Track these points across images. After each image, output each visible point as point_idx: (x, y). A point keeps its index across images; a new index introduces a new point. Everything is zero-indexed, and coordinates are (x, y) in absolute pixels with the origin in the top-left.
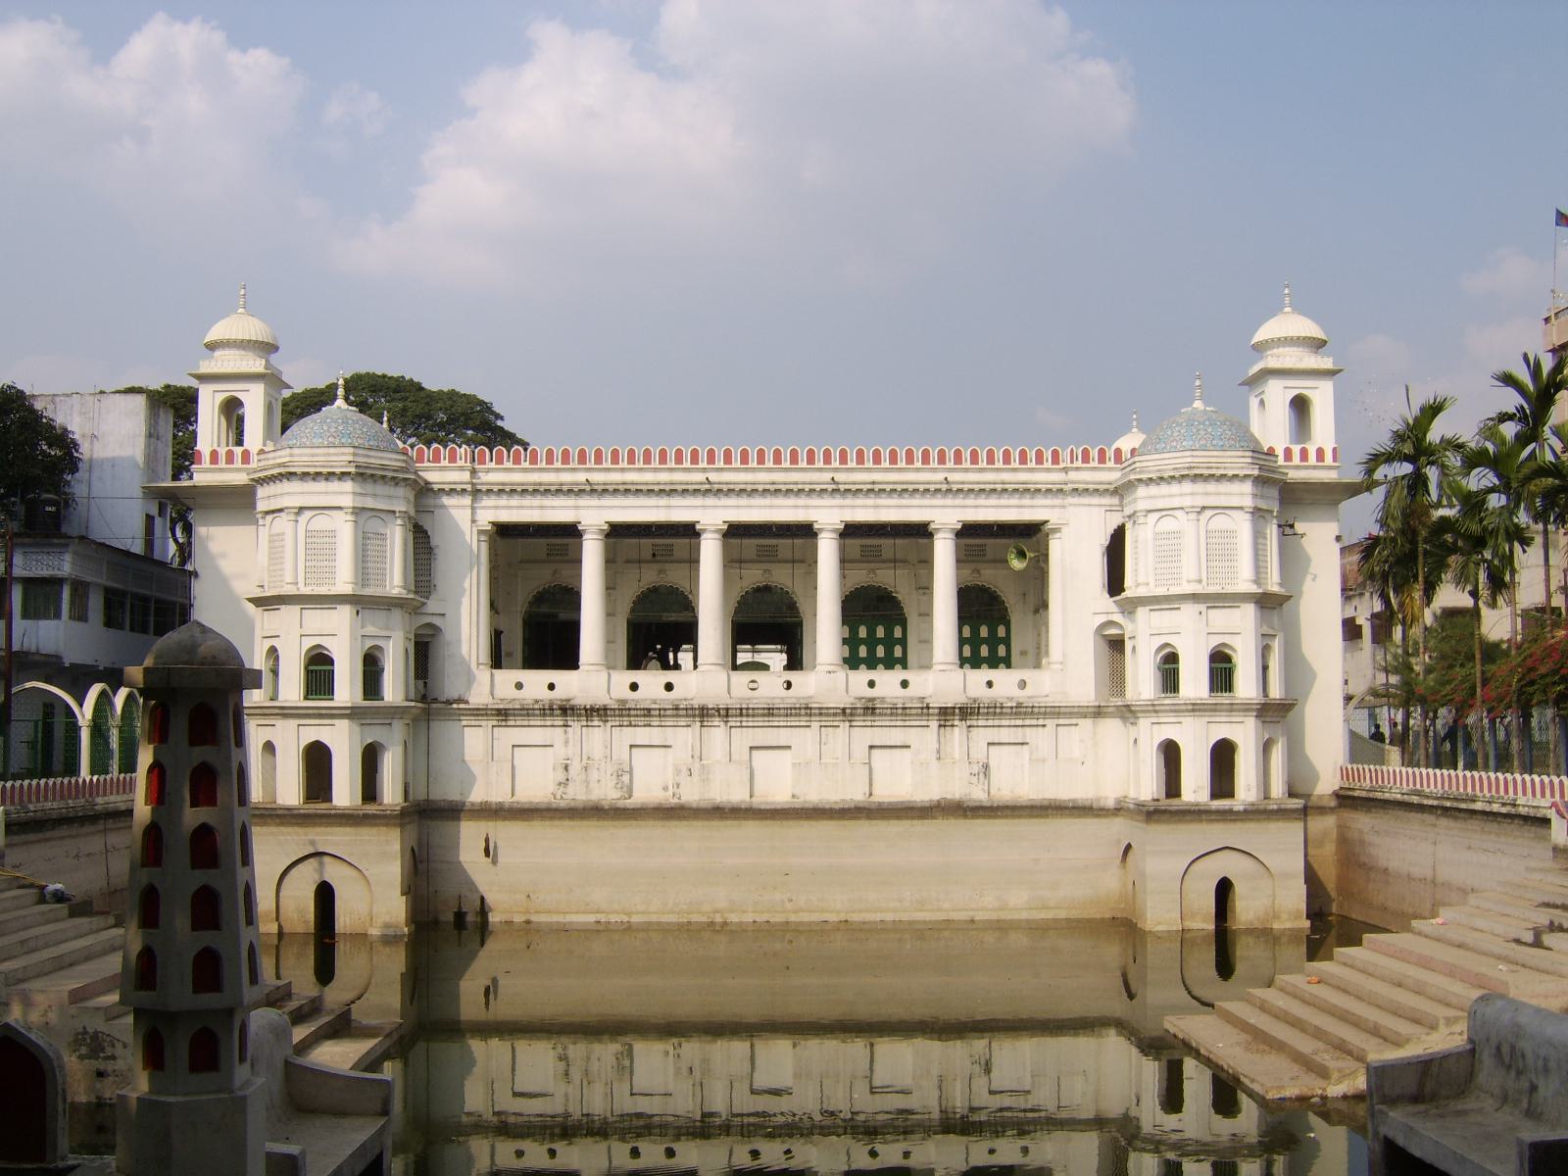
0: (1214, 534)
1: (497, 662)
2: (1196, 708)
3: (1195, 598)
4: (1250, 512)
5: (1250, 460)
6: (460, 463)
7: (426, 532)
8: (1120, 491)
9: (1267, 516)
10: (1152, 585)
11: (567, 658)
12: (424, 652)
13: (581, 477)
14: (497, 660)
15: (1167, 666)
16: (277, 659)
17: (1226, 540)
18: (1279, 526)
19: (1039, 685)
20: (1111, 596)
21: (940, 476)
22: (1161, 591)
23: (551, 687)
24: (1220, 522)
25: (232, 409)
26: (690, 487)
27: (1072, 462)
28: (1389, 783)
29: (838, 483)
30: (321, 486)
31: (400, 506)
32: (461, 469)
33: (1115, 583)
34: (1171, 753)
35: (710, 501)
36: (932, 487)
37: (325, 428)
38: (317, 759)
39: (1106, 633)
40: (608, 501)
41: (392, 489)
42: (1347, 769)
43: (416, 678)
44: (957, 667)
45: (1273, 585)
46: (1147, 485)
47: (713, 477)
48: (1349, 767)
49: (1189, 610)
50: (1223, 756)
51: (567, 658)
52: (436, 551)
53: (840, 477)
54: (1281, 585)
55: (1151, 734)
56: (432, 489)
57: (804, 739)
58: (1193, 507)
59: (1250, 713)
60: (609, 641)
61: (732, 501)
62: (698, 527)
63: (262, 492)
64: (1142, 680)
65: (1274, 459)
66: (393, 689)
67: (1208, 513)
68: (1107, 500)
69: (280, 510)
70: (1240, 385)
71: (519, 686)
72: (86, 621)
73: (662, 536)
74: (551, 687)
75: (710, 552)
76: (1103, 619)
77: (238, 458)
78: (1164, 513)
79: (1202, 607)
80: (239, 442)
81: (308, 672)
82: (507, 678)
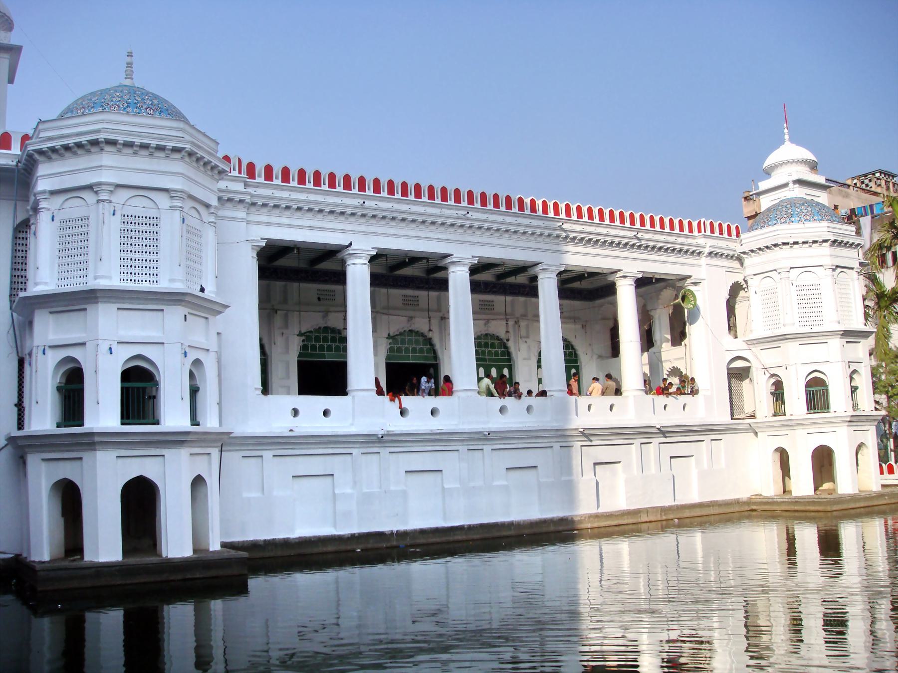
10: (798, 324)
15: (811, 389)
22: (807, 330)
23: (326, 413)
30: (142, 161)
39: (730, 367)
59: (872, 423)
63: (43, 169)
67: (839, 270)
69: (89, 187)
71: (296, 412)
73: (325, 282)
74: (326, 413)
81: (125, 392)
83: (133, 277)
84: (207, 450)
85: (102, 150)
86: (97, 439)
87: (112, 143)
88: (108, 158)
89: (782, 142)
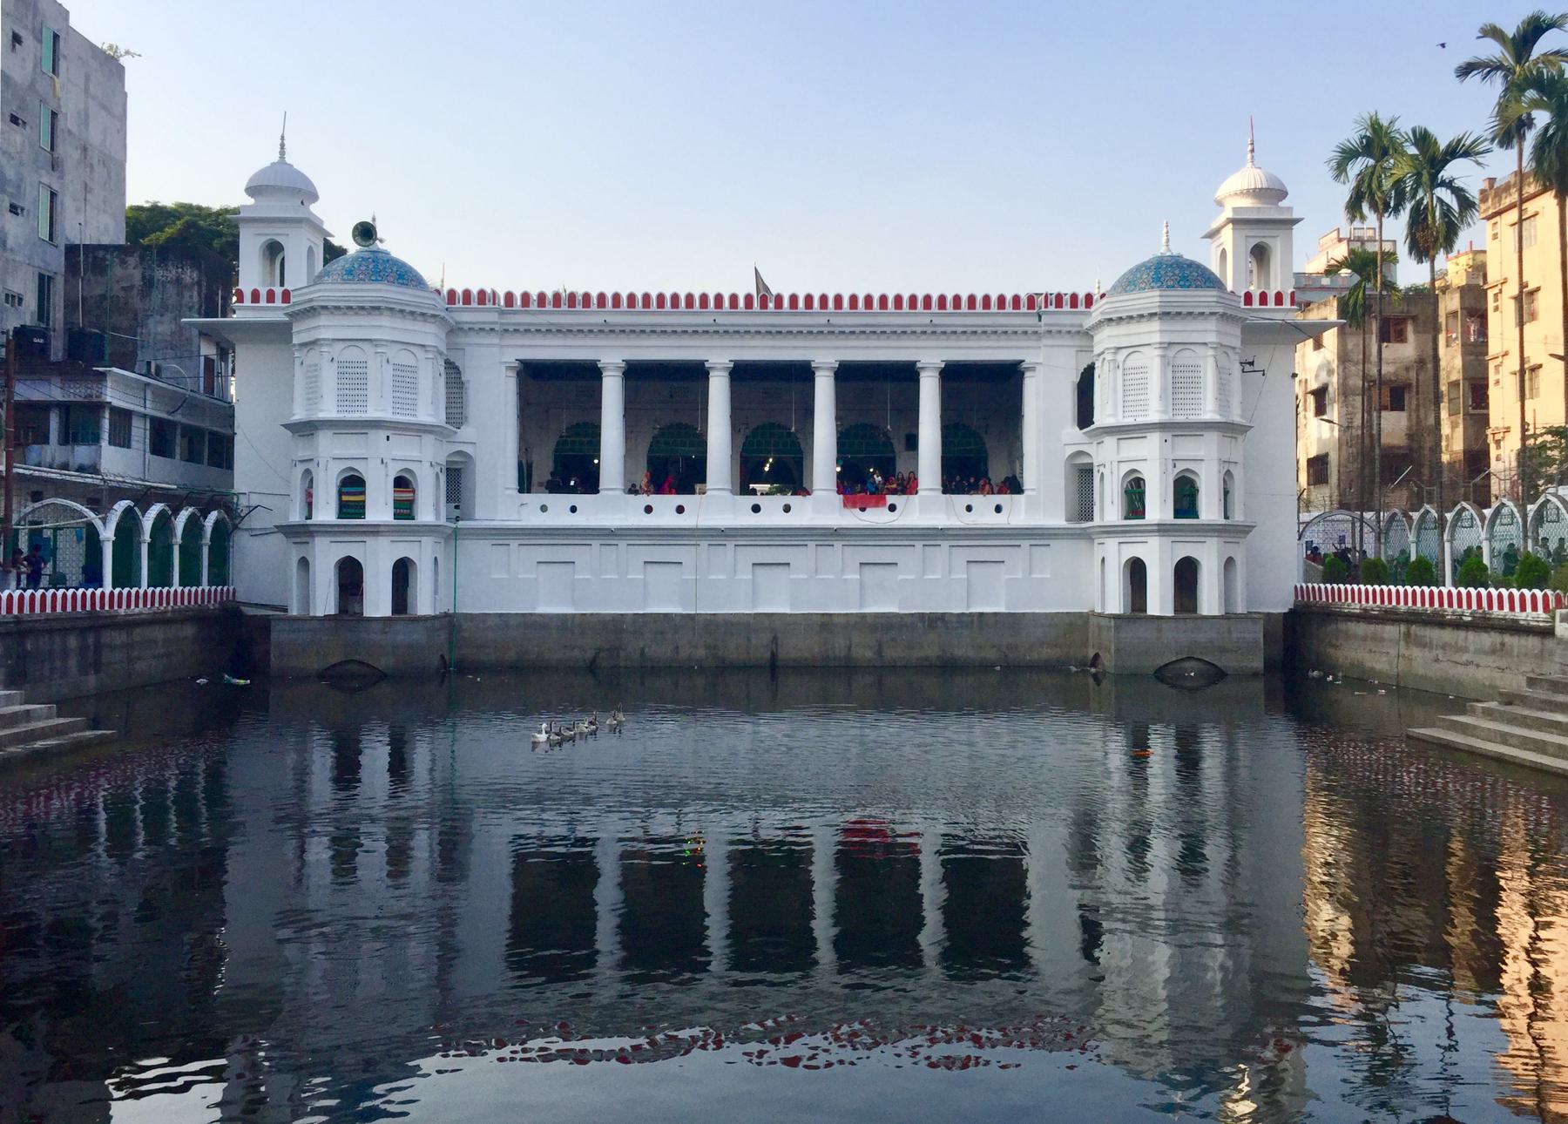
0: (1180, 369)
1: (525, 485)
2: (1162, 529)
3: (1162, 426)
4: (1215, 348)
5: (1215, 299)
6: (489, 305)
7: (457, 368)
8: (1087, 334)
9: (1230, 352)
11: (589, 482)
12: (456, 478)
13: (600, 319)
14: (525, 484)
16: (311, 481)
17: (1191, 374)
18: (1241, 363)
19: (1018, 512)
20: (1081, 429)
21: (927, 320)
23: (573, 509)
24: (1185, 358)
25: (274, 250)
26: (700, 329)
27: (1046, 306)
28: (1346, 599)
29: (834, 326)
31: (429, 341)
32: (489, 310)
33: (1085, 416)
34: (1136, 570)
35: (716, 342)
36: (919, 330)
37: (356, 266)
38: (350, 576)
40: (623, 341)
41: (420, 324)
42: (1301, 587)
43: (448, 501)
44: (939, 493)
45: (1236, 417)
46: (1118, 324)
47: (720, 320)
48: (1304, 586)
49: (1155, 438)
50: (1186, 573)
51: (589, 482)
52: (467, 385)
53: (834, 320)
54: (1242, 417)
55: (1116, 554)
56: (461, 329)
57: (802, 558)
58: (1161, 343)
60: (628, 470)
61: (736, 342)
62: (707, 365)
64: (1110, 509)
65: (1236, 298)
66: (426, 513)
68: (1077, 341)
69: (315, 342)
70: (1203, 237)
72: (129, 447)
74: (573, 509)
75: (719, 391)
76: (1070, 450)
77: (278, 297)
78: (1132, 350)
79: (1168, 436)
80: (282, 284)
82: (535, 499)
83: (347, 408)
84: (419, 539)
85: (320, 314)
86: (312, 529)
87: (325, 308)
88: (324, 320)
89: (1244, 165)
